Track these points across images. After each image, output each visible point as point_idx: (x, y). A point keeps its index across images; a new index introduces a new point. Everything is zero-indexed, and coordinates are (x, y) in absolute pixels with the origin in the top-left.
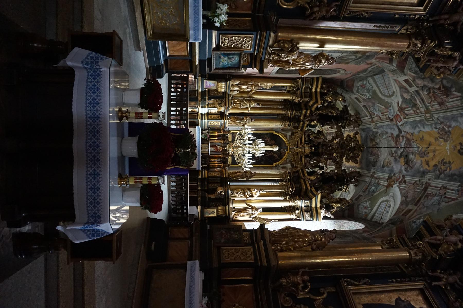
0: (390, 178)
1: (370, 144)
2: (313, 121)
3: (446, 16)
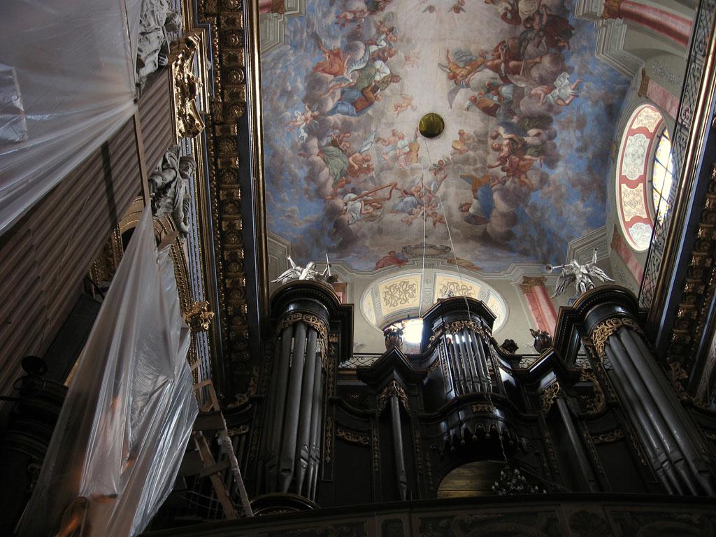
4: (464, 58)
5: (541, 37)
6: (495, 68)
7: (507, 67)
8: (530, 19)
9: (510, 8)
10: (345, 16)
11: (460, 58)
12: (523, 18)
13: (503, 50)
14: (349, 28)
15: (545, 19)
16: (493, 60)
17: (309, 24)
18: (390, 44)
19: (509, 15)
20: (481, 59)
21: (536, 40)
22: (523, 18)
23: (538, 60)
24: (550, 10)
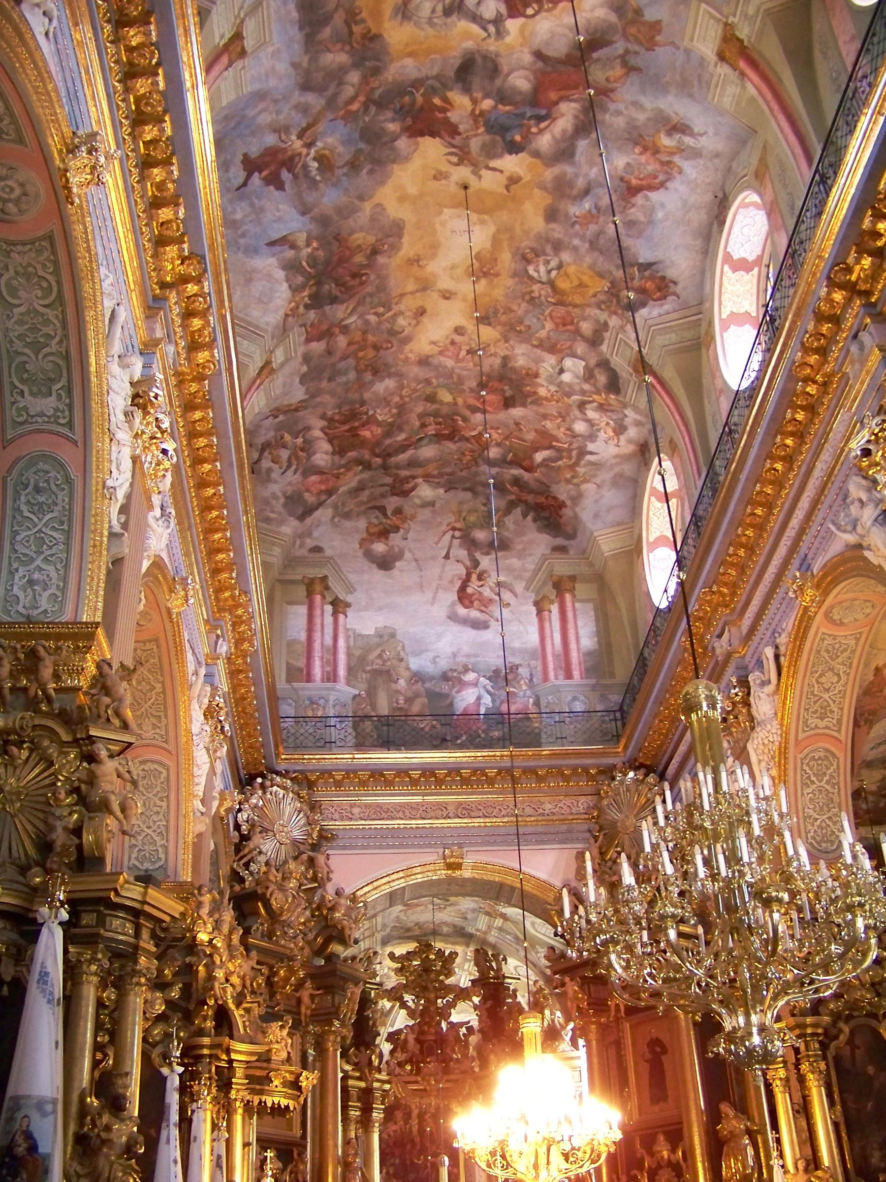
0: (488, 914)
1: (417, 932)
2: (370, 1062)
3: (303, 1010)
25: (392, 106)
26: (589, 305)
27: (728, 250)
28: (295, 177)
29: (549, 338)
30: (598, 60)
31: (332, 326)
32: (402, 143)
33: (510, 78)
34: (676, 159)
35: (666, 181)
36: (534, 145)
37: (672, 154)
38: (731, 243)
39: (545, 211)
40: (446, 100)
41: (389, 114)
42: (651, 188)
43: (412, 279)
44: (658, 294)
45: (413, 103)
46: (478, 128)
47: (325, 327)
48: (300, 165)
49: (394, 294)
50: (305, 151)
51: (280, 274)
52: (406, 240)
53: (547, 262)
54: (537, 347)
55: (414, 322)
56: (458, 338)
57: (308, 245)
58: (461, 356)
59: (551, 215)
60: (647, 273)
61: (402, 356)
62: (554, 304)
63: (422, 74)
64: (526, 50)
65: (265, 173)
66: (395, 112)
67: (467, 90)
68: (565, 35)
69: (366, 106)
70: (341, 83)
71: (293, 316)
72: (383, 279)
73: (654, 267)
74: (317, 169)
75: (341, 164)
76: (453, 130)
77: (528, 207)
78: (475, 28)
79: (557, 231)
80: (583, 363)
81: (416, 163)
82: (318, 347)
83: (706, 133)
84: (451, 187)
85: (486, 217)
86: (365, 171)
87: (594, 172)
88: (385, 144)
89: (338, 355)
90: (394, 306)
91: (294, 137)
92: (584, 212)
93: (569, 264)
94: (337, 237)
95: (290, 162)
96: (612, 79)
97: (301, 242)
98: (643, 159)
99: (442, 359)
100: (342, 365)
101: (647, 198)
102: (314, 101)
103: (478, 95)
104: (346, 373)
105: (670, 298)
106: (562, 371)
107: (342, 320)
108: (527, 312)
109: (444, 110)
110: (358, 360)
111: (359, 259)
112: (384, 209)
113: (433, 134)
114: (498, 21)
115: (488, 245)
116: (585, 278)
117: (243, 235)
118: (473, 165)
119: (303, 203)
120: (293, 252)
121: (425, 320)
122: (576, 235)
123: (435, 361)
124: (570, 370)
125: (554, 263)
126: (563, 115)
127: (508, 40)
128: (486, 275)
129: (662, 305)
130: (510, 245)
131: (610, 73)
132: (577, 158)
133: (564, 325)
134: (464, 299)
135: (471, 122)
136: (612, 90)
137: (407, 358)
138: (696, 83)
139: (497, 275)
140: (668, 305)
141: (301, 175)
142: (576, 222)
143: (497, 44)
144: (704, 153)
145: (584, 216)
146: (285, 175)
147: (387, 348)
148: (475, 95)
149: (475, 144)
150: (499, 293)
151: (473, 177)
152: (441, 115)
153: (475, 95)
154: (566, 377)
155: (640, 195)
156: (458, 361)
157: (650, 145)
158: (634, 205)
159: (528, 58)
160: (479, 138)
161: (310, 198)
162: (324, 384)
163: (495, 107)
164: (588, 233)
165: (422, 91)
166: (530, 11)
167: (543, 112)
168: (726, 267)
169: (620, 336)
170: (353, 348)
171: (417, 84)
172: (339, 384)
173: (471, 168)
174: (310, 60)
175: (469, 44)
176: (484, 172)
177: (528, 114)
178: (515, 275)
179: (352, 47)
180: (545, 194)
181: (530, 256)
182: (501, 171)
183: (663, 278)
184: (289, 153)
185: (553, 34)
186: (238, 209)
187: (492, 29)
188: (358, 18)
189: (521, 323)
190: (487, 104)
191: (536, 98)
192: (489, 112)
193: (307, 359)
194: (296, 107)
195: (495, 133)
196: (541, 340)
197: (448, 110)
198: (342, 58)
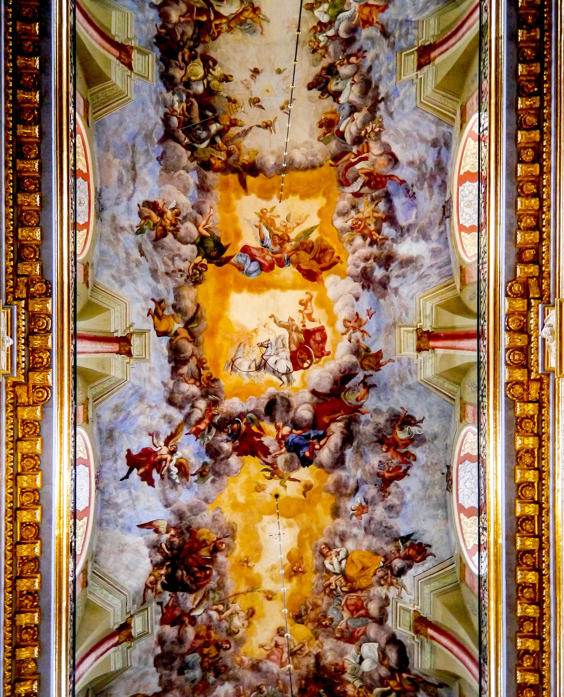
4: (247, 27)
5: (181, 40)
6: (218, 16)
7: (209, 16)
8: (193, 58)
9: (211, 70)
10: (357, 58)
11: (250, 27)
12: (198, 60)
13: (214, 33)
14: (355, 48)
15: (180, 58)
16: (221, 24)
17: (392, 46)
18: (315, 38)
19: (211, 63)
20: (232, 25)
21: (185, 38)
22: (198, 60)
23: (182, 19)
24: (176, 64)
25: (226, 430)
26: (371, 586)
27: (460, 502)
28: (162, 477)
29: (347, 627)
30: (349, 388)
31: (184, 613)
32: (234, 460)
33: (299, 410)
34: (411, 449)
35: (408, 468)
36: (318, 458)
37: (406, 445)
38: (460, 496)
39: (332, 509)
40: (260, 428)
41: (224, 436)
42: (400, 477)
43: (243, 580)
44: (419, 558)
45: (240, 428)
46: (281, 448)
47: (177, 613)
48: (166, 468)
49: (231, 593)
50: (169, 457)
51: (146, 551)
52: (237, 541)
53: (338, 554)
54: (338, 639)
55: (246, 623)
56: (281, 641)
57: (167, 532)
58: (283, 660)
59: (336, 513)
60: (408, 544)
61: (238, 659)
62: (347, 592)
63: (244, 410)
64: (306, 390)
65: (142, 470)
66: (229, 435)
67: (273, 420)
68: (329, 377)
69: (210, 427)
70: (193, 407)
71: (152, 589)
72: (222, 575)
73: (413, 538)
74: (177, 474)
75: (193, 472)
76: (266, 451)
77: (319, 508)
78: (275, 379)
79: (341, 524)
80: (376, 645)
81: (243, 478)
82: (171, 632)
83: (424, 418)
84: (267, 496)
85: (292, 520)
86: (209, 480)
87: (359, 474)
88: (222, 460)
89: (187, 646)
90: (230, 605)
91: (162, 444)
92: (357, 505)
93: (353, 552)
94: (189, 528)
95: (159, 465)
96: (359, 399)
97: (163, 529)
98: (389, 454)
99: (270, 663)
100: (190, 658)
101: (397, 486)
102: (178, 416)
103: (280, 424)
104: (193, 668)
105: (429, 558)
106: (362, 659)
107: (192, 610)
108: (329, 605)
109: (259, 436)
110: (203, 656)
111: (204, 553)
112: (222, 512)
113: (254, 454)
114: (287, 374)
115: (295, 545)
116: (366, 561)
117: (122, 516)
118: (280, 478)
119: (166, 499)
120: (156, 535)
121: (254, 621)
122: (355, 524)
123: (264, 667)
124: (368, 657)
125: (342, 555)
126: (334, 433)
127: (295, 385)
128: (296, 572)
129: (423, 564)
130: (311, 543)
131: (358, 394)
132: (347, 464)
133: (357, 610)
134: (283, 599)
135: (277, 444)
136: (361, 406)
137: (242, 661)
138: (409, 376)
139: (303, 572)
140: (429, 562)
141: (166, 477)
142: (353, 514)
143: (289, 388)
144: (427, 437)
145: (357, 509)
146: (155, 475)
147: (226, 649)
148: (278, 424)
149: (280, 461)
150: (307, 590)
151: (282, 488)
152: (258, 439)
153: (278, 424)
154: (366, 666)
155: (392, 485)
156: (282, 665)
157: (391, 441)
158: (389, 493)
159: (308, 396)
160: (283, 456)
161: (172, 495)
162: (174, 676)
163: (291, 432)
164: (363, 522)
165: (245, 421)
166: (306, 365)
167: (321, 432)
168: (462, 515)
169: (399, 604)
170: (200, 642)
171: (242, 415)
172: (187, 680)
173: (279, 481)
174: (174, 383)
175: (272, 390)
176: (288, 483)
177: (312, 436)
178: (317, 571)
179: (201, 384)
180: (329, 495)
181: (325, 551)
182: (299, 481)
183: (420, 544)
184: (159, 457)
185: (321, 378)
186: (120, 494)
187: (284, 378)
188: (204, 365)
189: (325, 616)
190: (286, 430)
191: (315, 423)
192: (288, 436)
193: (161, 641)
194: (165, 417)
195: (292, 452)
196: (342, 631)
197: (262, 436)
198: (194, 389)
